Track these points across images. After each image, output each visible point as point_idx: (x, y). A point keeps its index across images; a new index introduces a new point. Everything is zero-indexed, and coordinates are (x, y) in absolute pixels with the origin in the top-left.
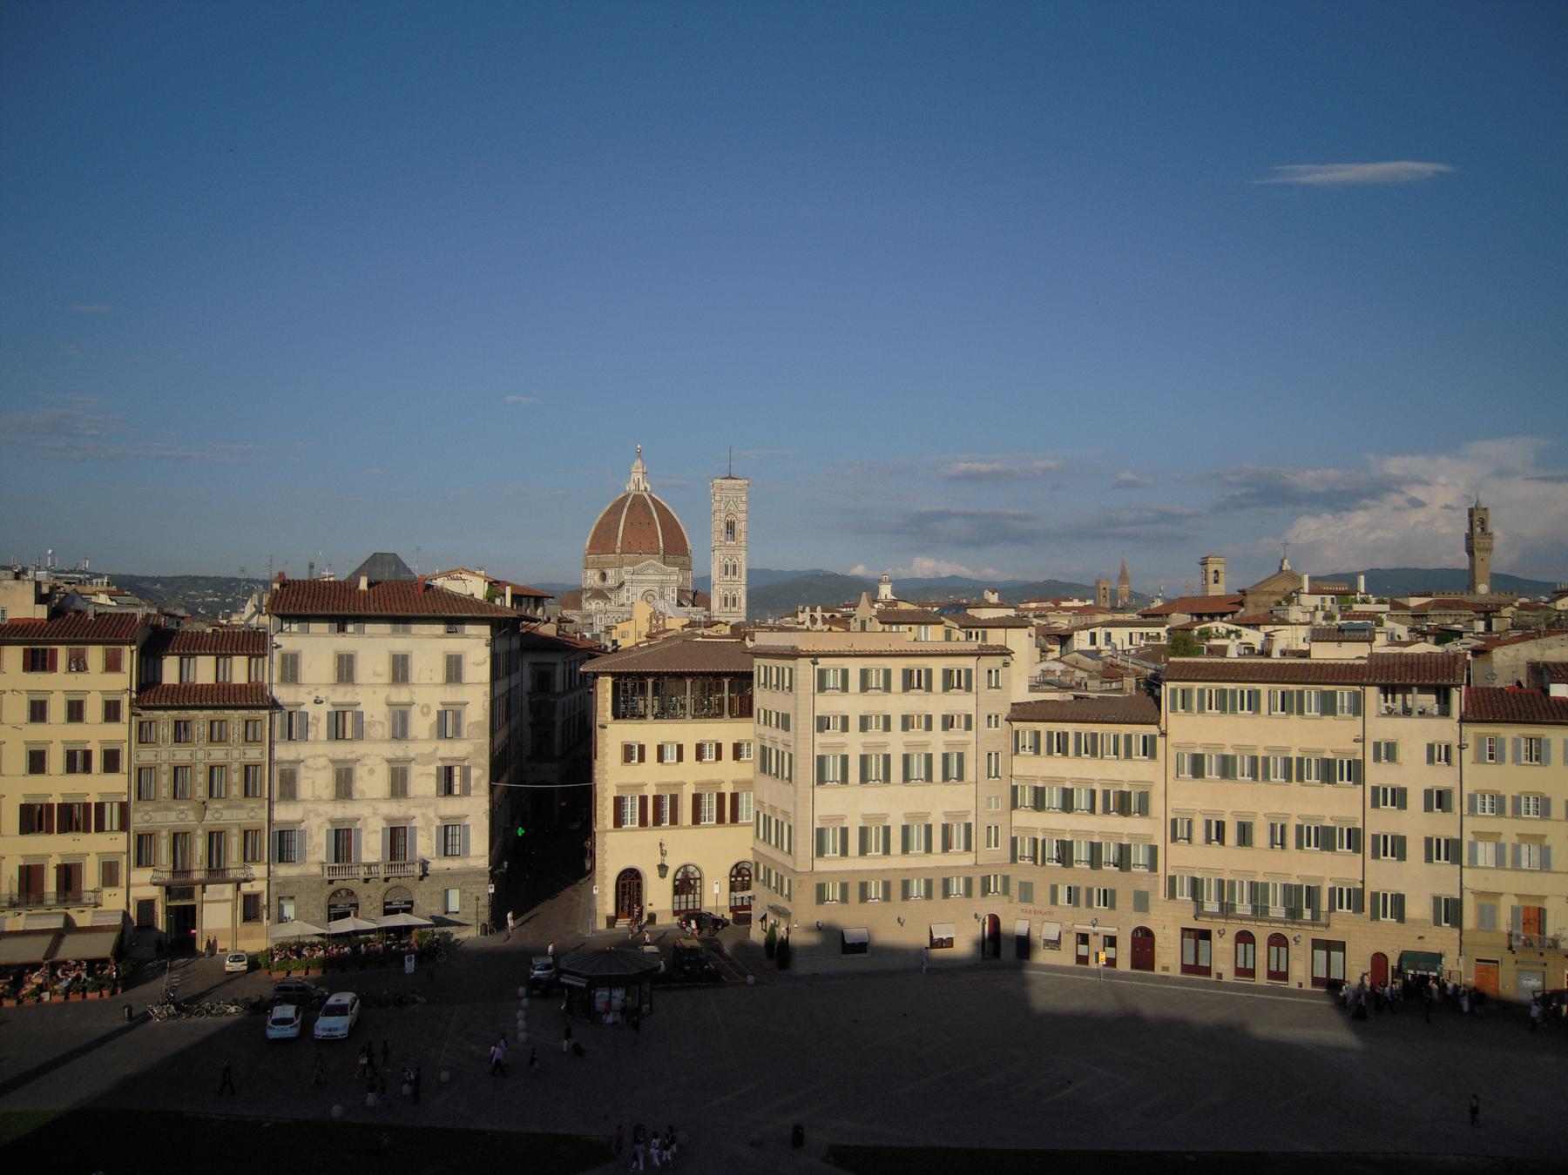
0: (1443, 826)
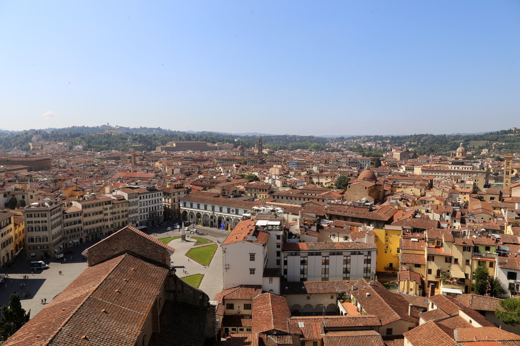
0: (111, 216)
